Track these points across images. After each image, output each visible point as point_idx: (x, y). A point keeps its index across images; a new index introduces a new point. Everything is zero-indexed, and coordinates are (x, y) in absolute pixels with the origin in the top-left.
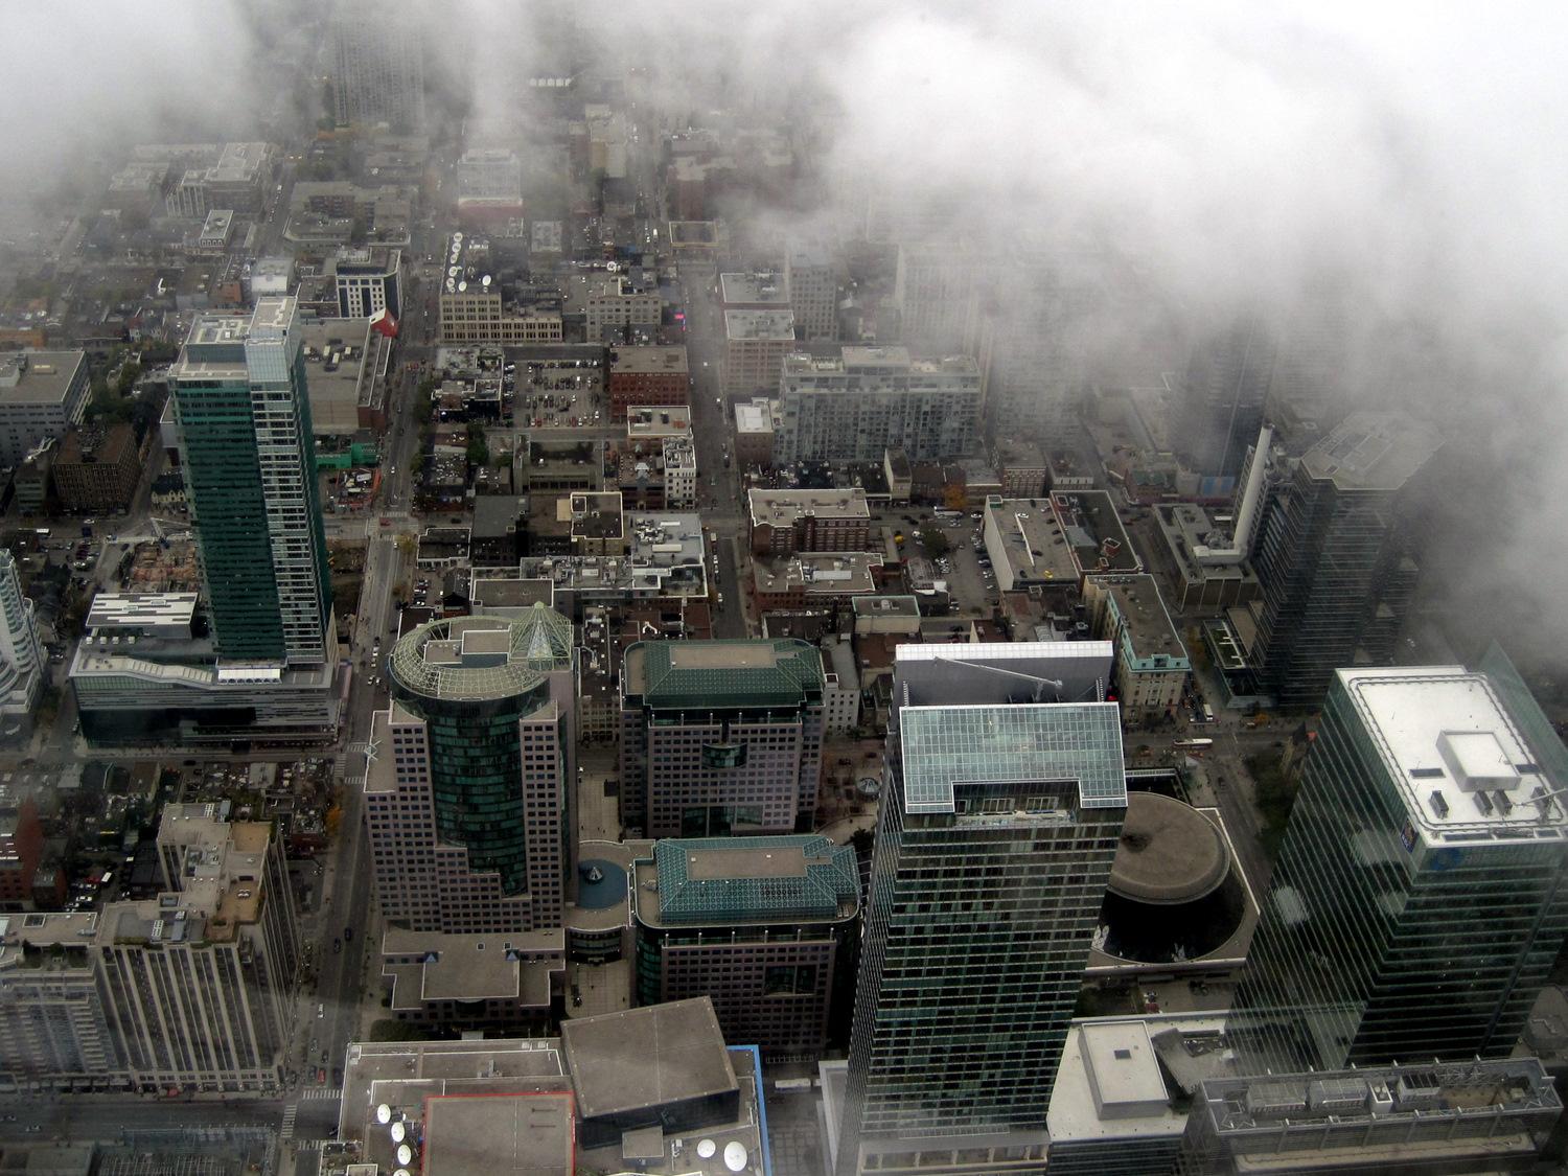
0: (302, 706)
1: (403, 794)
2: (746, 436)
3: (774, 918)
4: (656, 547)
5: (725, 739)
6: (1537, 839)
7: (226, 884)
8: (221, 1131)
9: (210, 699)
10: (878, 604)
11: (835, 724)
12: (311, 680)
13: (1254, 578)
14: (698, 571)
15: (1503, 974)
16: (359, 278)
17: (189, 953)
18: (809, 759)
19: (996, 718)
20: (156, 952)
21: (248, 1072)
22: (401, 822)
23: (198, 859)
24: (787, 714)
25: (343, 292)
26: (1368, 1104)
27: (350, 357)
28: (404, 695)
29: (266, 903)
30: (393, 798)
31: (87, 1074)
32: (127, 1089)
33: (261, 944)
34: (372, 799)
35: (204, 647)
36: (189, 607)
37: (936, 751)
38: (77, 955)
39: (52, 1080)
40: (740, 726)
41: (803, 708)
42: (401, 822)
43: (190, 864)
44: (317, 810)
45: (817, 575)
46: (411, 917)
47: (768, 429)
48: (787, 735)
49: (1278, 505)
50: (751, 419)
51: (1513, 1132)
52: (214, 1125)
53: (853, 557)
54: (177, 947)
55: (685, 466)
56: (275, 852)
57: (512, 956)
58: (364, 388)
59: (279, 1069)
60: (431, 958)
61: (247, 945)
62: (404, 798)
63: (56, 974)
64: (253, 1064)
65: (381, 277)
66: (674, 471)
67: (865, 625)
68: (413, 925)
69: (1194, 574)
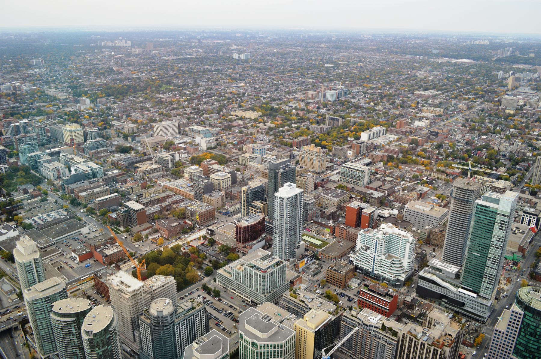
0: (479, 308)
7: (444, 333)
9: (453, 295)
12: (484, 302)
16: (529, 216)
17: (426, 345)
22: (503, 342)
23: (438, 323)
25: (523, 218)
27: (520, 233)
28: (520, 302)
30: (503, 333)
34: (496, 331)
35: (456, 282)
36: (457, 270)
38: (395, 334)
42: (503, 342)
54: (424, 342)
56: (461, 333)
58: (523, 241)
62: (507, 335)
63: (387, 335)
65: (536, 217)
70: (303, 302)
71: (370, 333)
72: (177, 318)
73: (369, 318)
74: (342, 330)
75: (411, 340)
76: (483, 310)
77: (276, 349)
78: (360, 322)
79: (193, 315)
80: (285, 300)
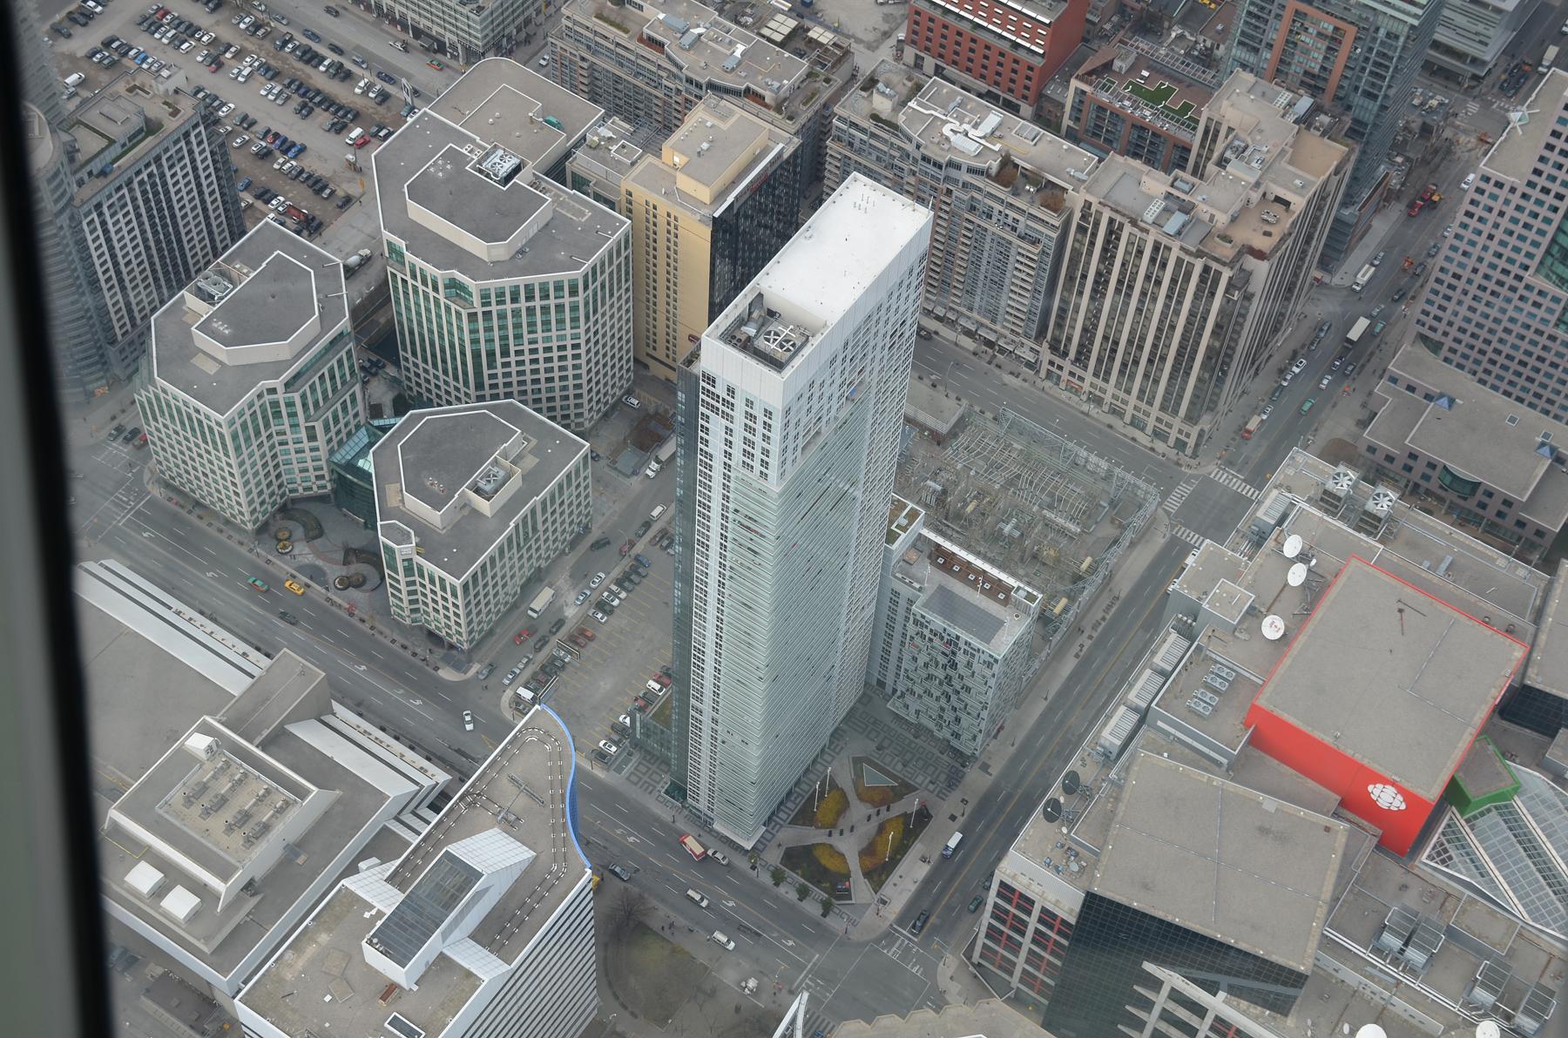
0: (1460, 20)
1: (1529, 191)
8: (1104, 465)
17: (1175, 253)
20: (1139, 234)
21: (1166, 417)
23: (1240, 152)
29: (1290, 241)
30: (1513, 190)
31: (998, 327)
32: (1029, 365)
33: (1258, 283)
38: (1051, 195)
39: (961, 314)
43: (1228, 154)
44: (1407, 159)
46: (1448, 342)
52: (1100, 455)
54: (1165, 241)
56: (1332, 188)
57: (1546, 450)
59: (1201, 434)
60: (1444, 401)
61: (1241, 281)
64: (1175, 412)
68: (1444, 352)
70: (657, 45)
71: (949, 192)
72: (80, 183)
73: (946, 130)
74: (830, 166)
75: (1113, 233)
76: (1480, 28)
77: (552, 302)
78: (909, 147)
79: (158, 159)
80: (571, 34)
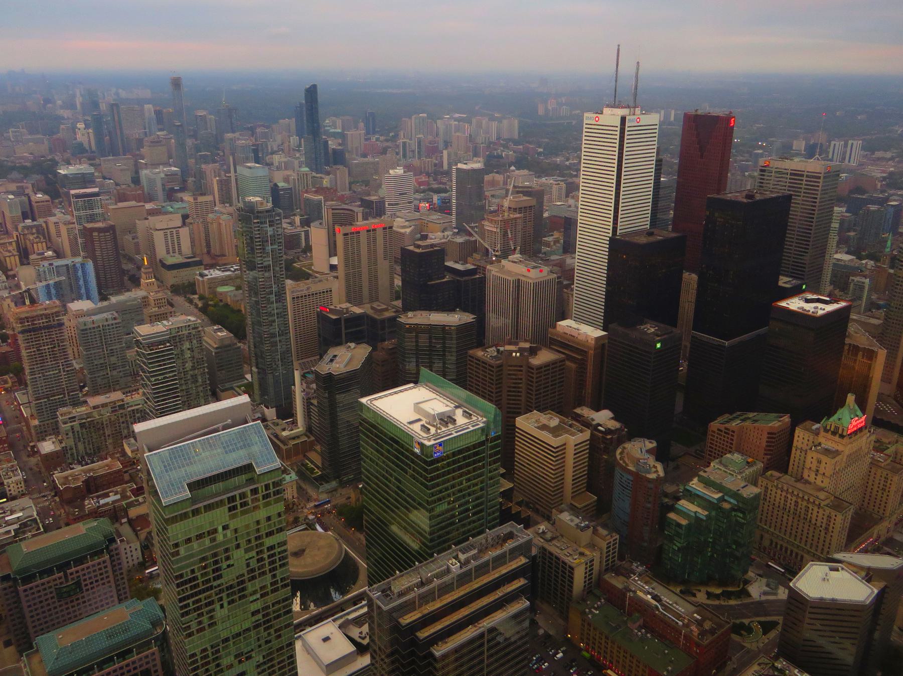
2: (46, 455)
3: (118, 649)
4: (7, 519)
5: (67, 581)
6: (472, 429)
10: (138, 501)
11: (131, 564)
13: (313, 438)
14: (35, 519)
15: (481, 504)
18: (120, 582)
19: (199, 445)
24: (99, 553)
26: (448, 571)
37: (171, 470)
40: (73, 570)
41: (107, 548)
45: (102, 502)
47: (59, 448)
48: (102, 566)
49: (312, 404)
50: (48, 447)
51: (516, 558)
53: (118, 488)
55: (15, 476)
66: (10, 481)
67: (133, 513)
69: (285, 443)
